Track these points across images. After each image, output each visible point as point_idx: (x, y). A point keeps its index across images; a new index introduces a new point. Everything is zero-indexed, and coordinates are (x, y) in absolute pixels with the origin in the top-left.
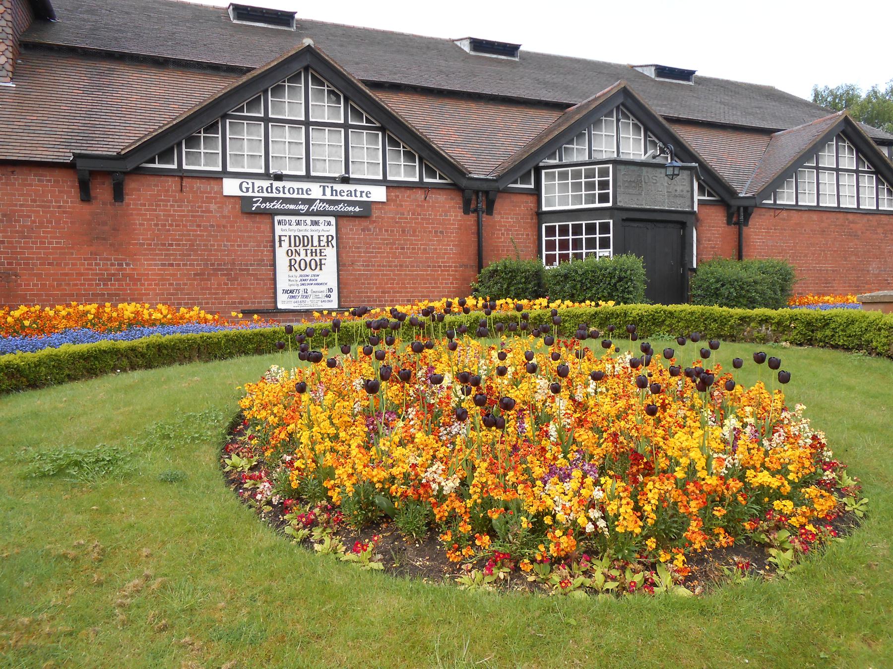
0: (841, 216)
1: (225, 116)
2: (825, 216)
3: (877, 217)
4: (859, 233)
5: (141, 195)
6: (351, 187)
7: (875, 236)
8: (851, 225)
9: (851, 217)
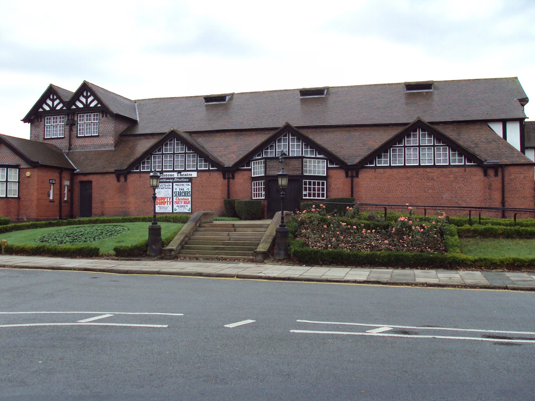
0: (422, 169)
1: (152, 154)
2: (409, 170)
3: (449, 169)
4: (435, 178)
5: (131, 178)
6: (186, 173)
7: (447, 179)
8: (429, 174)
9: (428, 170)
